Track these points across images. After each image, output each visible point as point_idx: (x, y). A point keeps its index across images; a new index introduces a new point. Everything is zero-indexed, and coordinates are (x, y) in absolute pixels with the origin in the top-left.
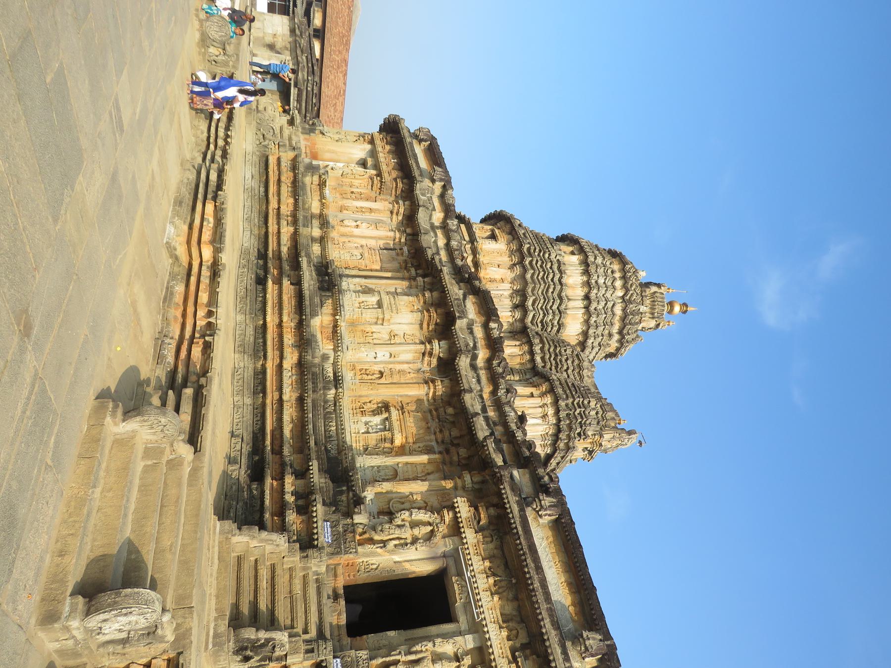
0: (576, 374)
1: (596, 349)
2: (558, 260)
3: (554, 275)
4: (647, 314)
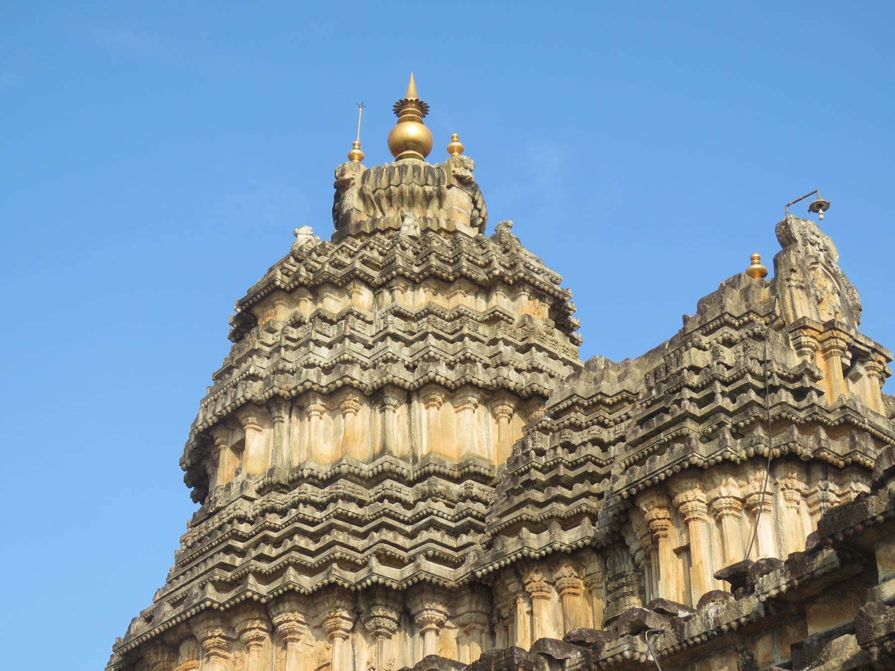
0: (615, 416)
1: (539, 358)
2: (260, 491)
3: (306, 502)
4: (429, 214)
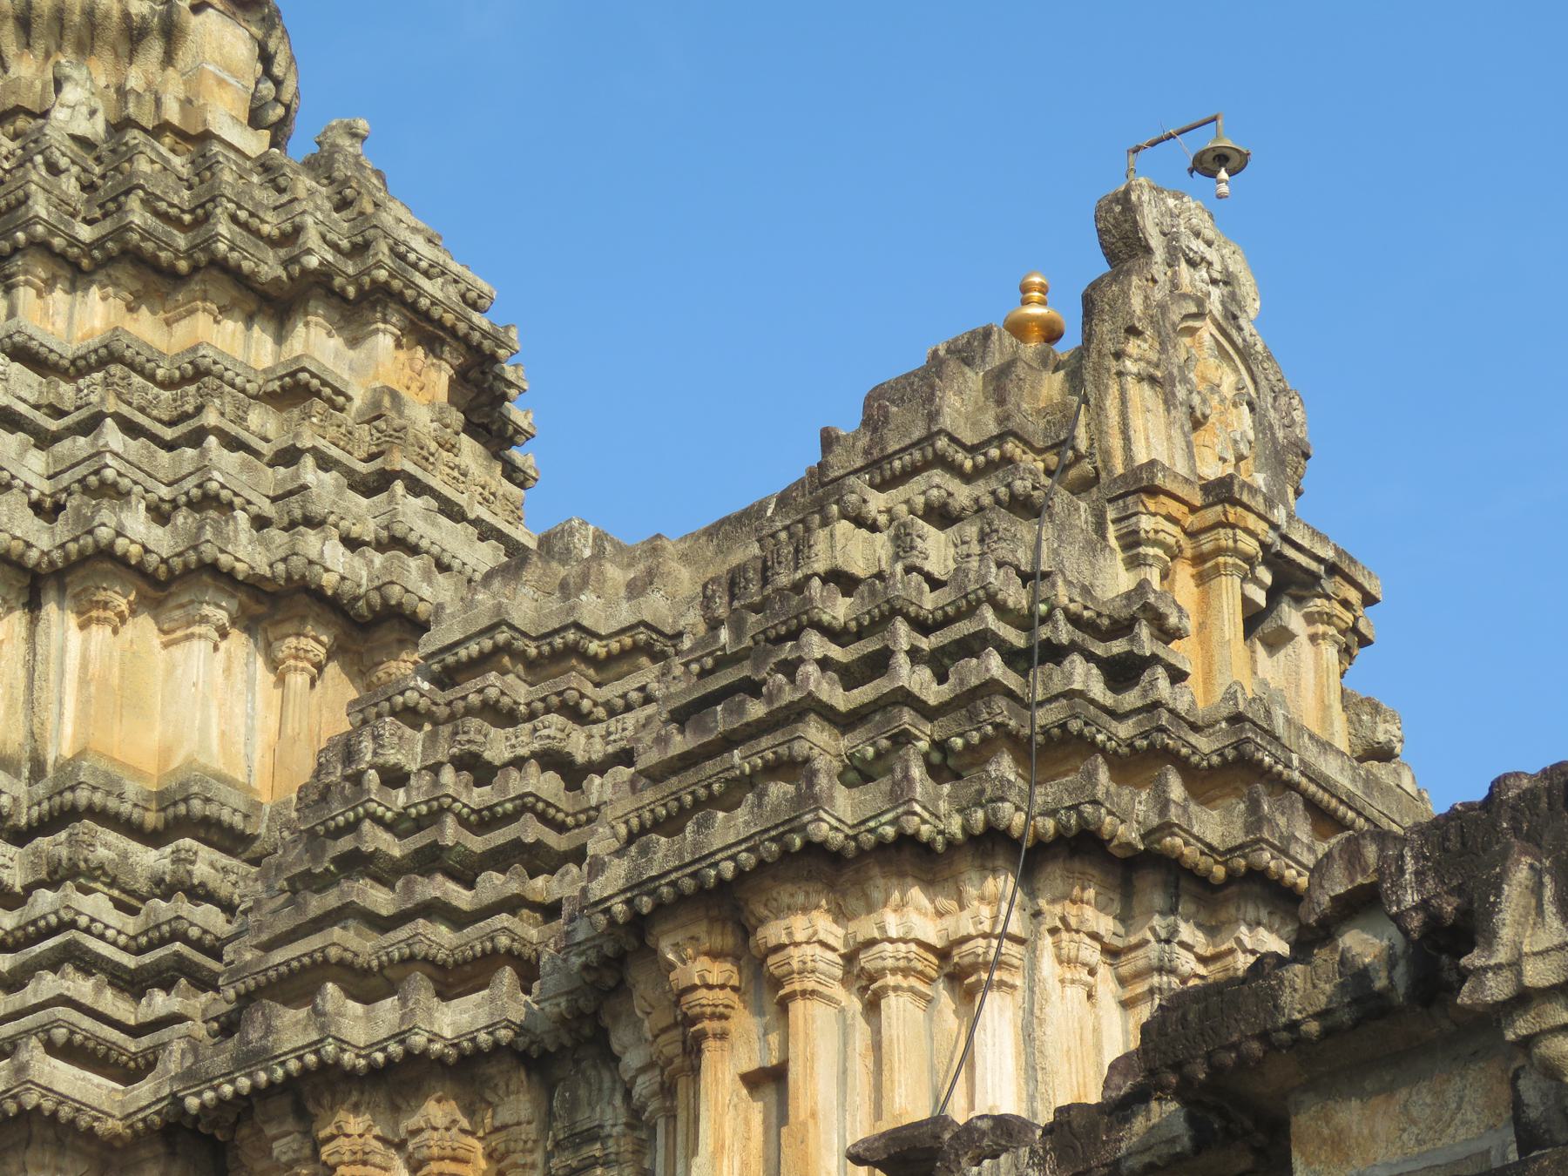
0: (611, 692)
1: (413, 513)
4: (135, 79)
